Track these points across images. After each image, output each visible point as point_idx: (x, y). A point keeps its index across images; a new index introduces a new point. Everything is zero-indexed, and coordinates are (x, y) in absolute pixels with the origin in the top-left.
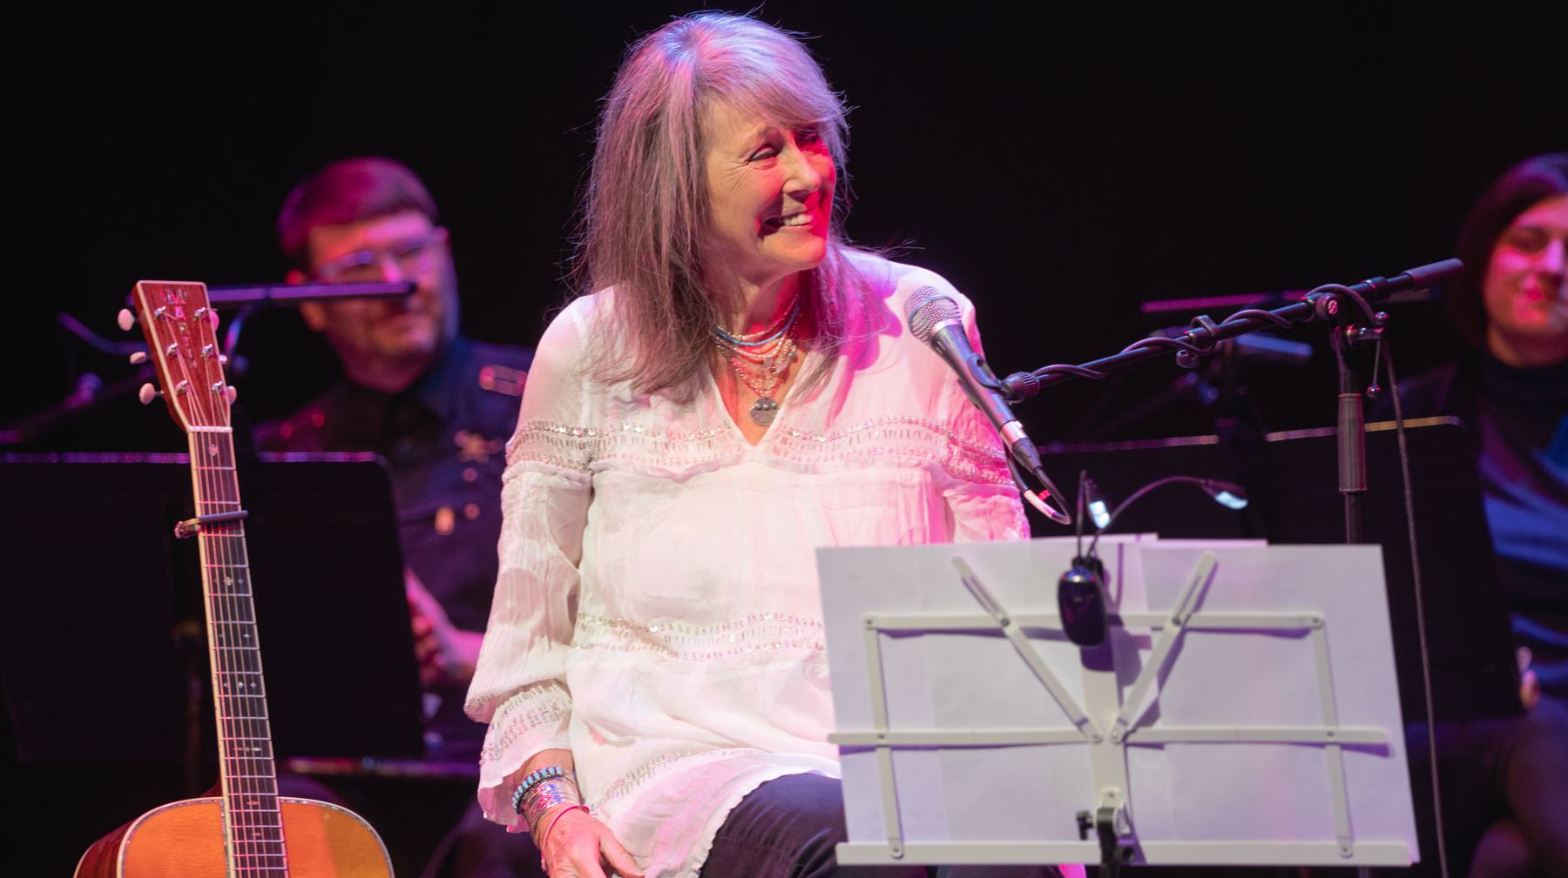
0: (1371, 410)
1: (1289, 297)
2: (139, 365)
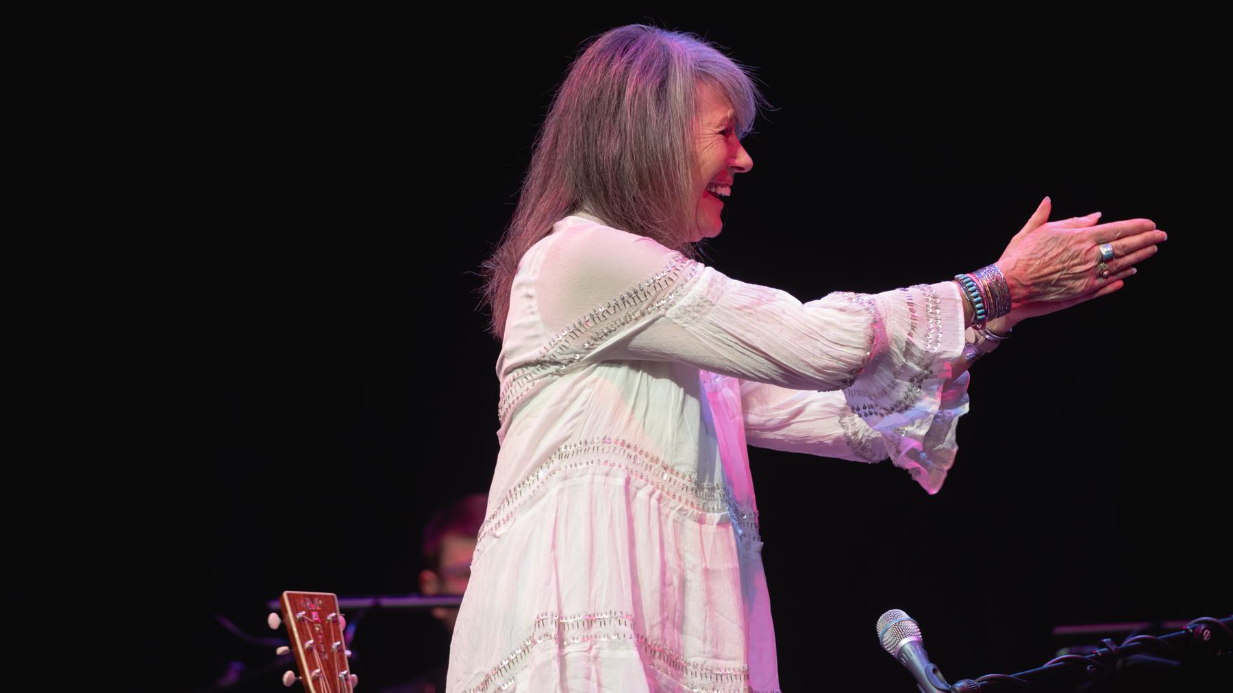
1: (1171, 625)
2: (283, 656)
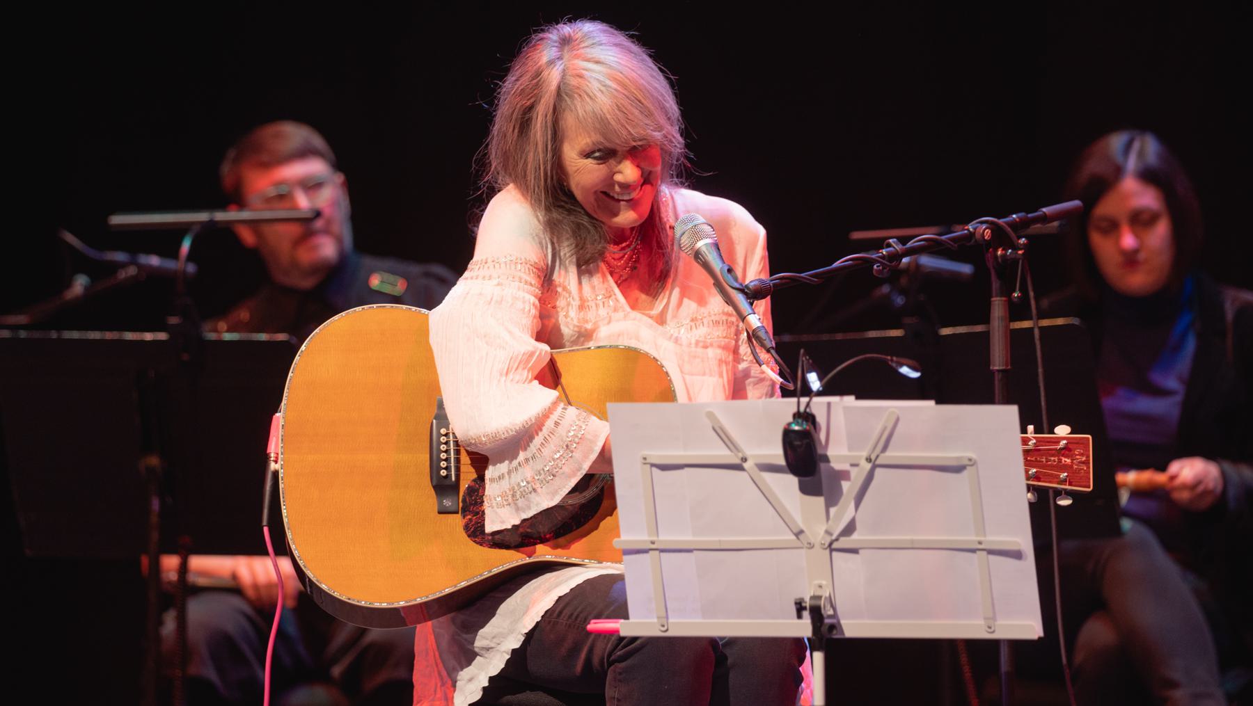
0: (1017, 311)
1: (958, 227)
